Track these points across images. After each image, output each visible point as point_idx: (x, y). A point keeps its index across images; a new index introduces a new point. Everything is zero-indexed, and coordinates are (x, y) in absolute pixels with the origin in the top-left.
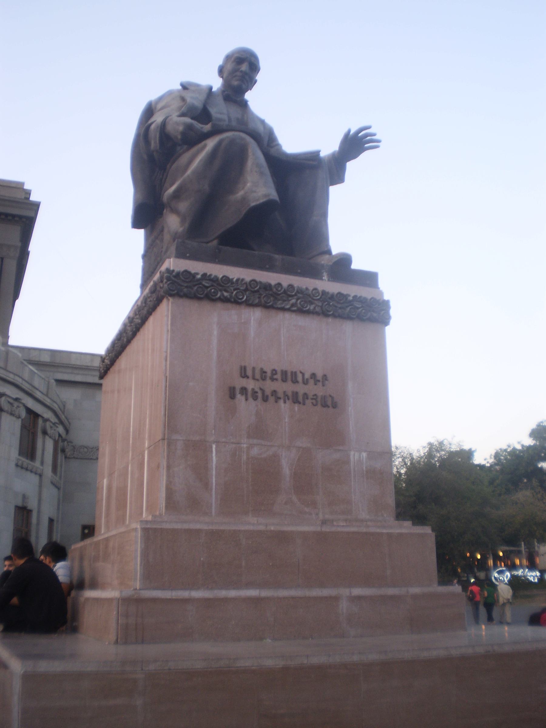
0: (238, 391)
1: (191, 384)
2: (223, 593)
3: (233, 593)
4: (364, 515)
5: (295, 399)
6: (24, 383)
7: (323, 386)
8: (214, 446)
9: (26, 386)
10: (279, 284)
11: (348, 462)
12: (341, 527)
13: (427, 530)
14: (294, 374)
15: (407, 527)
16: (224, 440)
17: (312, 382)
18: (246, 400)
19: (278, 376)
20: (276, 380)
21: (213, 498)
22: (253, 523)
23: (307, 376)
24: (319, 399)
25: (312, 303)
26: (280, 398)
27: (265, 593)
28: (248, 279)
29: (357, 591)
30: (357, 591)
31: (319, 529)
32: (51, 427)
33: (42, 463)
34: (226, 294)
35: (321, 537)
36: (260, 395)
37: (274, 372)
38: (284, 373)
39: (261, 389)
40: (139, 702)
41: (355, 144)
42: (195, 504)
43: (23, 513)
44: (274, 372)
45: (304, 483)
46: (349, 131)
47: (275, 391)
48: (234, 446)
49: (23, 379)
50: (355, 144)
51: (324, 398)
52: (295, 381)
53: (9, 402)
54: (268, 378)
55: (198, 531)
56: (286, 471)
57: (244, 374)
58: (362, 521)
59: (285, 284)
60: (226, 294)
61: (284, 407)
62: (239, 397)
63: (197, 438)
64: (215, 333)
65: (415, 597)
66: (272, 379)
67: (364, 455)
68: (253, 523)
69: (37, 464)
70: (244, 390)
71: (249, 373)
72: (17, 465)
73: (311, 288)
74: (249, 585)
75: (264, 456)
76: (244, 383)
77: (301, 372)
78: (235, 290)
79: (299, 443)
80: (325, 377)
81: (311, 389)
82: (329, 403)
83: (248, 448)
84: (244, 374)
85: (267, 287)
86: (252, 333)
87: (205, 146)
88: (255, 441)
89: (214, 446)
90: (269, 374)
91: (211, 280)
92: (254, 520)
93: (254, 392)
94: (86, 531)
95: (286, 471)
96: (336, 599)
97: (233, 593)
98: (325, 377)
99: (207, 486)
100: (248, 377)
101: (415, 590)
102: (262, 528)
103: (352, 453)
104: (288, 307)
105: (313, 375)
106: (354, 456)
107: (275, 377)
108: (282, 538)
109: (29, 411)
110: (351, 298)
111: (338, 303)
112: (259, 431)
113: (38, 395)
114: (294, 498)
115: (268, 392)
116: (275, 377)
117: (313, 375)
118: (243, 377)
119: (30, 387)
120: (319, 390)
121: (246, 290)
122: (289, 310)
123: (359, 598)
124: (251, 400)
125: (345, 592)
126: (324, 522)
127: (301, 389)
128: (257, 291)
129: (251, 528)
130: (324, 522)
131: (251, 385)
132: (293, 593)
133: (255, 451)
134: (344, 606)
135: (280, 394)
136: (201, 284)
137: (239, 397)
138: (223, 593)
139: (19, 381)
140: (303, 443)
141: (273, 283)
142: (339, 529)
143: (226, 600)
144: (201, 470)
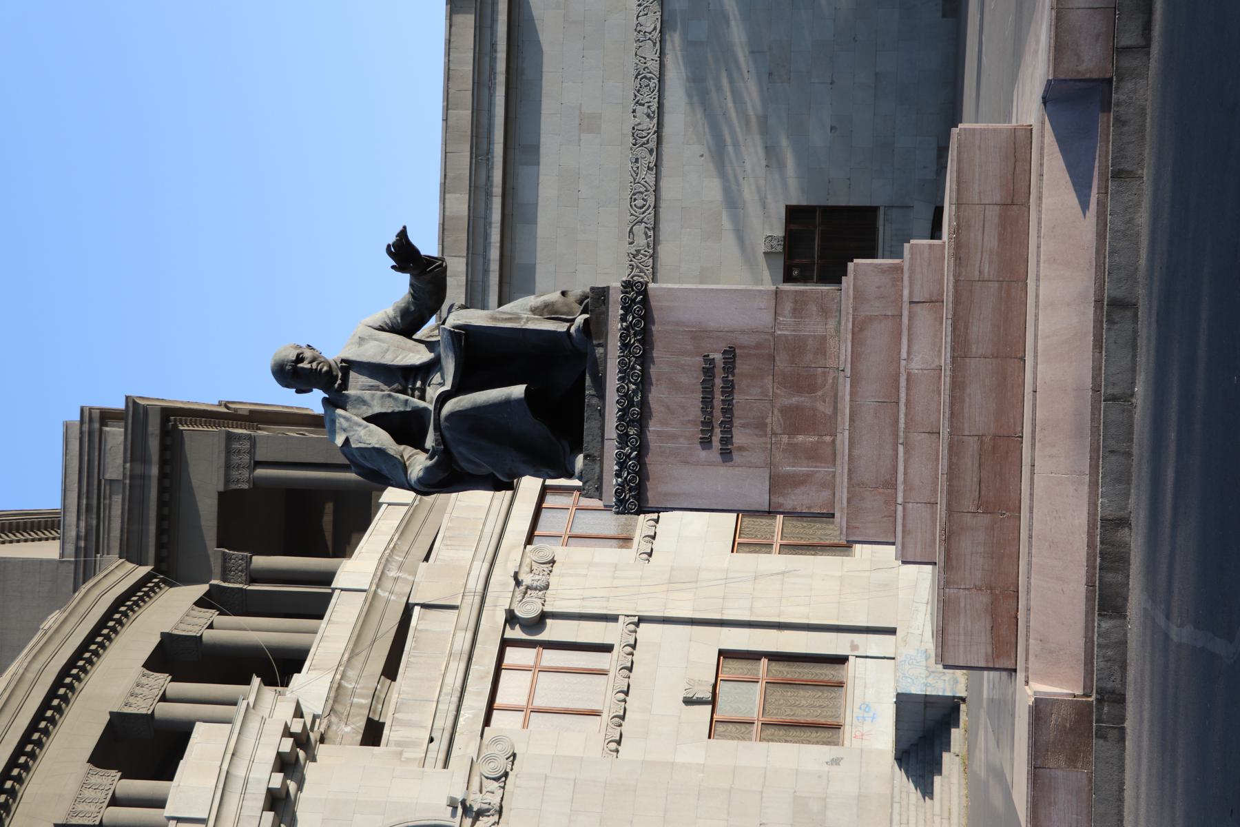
5: (729, 388)
12: (846, 349)
21: (822, 470)
22: (843, 438)
29: (904, 355)
31: (848, 380)
56: (794, 400)
88: (769, 429)
94: (795, 273)
95: (794, 400)
96: (909, 375)
102: (847, 433)
112: (760, 426)
114: (820, 393)
123: (909, 353)
127: (718, 382)
140: (768, 381)
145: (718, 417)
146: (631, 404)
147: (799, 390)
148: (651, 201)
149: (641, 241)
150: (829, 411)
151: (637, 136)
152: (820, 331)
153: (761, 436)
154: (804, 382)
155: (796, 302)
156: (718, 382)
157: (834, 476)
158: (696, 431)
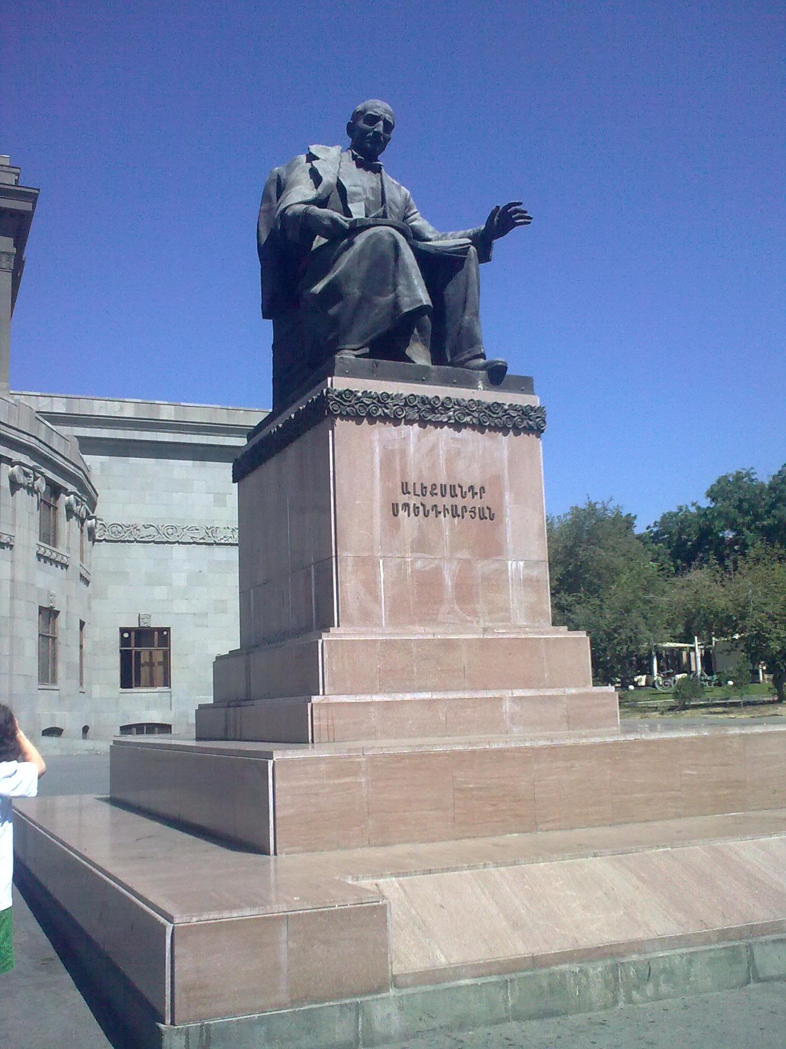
0: (400, 509)
1: (357, 502)
2: (399, 697)
3: (408, 697)
4: (522, 622)
6: (42, 445)
7: (481, 498)
8: (381, 561)
9: (45, 450)
10: (437, 397)
11: (507, 571)
12: (502, 633)
13: (582, 634)
14: (453, 487)
15: (563, 632)
16: (390, 555)
17: (470, 494)
18: (409, 515)
19: (438, 491)
20: (436, 494)
22: (420, 633)
23: (465, 489)
24: (477, 511)
25: (469, 415)
26: (440, 513)
27: (436, 696)
28: (406, 394)
29: (518, 693)
30: (518, 693)
31: (481, 636)
32: (77, 502)
33: (68, 548)
34: (386, 411)
35: (484, 644)
36: (421, 508)
37: (434, 486)
38: (443, 487)
39: (422, 505)
40: (363, 780)
41: (504, 221)
42: (367, 617)
43: (49, 614)
44: (434, 486)
45: (465, 593)
46: (498, 207)
47: (436, 506)
48: (399, 560)
49: (40, 441)
50: (504, 221)
51: (481, 510)
52: (454, 495)
53: (24, 472)
54: (428, 493)
55: (375, 641)
56: (448, 581)
57: (405, 492)
58: (520, 627)
59: (442, 397)
60: (386, 411)
61: (445, 520)
62: (402, 514)
63: (366, 554)
64: (377, 450)
65: (572, 697)
66: (432, 494)
67: (521, 564)
68: (420, 633)
69: (61, 549)
70: (406, 506)
71: (411, 489)
72: (38, 555)
73: (467, 399)
74: (420, 689)
75: (428, 568)
76: (404, 499)
77: (461, 487)
78: (394, 405)
79: (459, 556)
80: (482, 489)
81: (469, 502)
82: (487, 515)
83: (413, 562)
84: (405, 492)
85: (424, 400)
86: (412, 449)
87: (351, 244)
88: (419, 555)
89: (381, 561)
90: (429, 489)
91: (371, 397)
92: (421, 629)
93: (416, 508)
94: (126, 635)
95: (448, 581)
97: (408, 697)
98: (482, 489)
99: (376, 599)
100: (409, 493)
101: (573, 691)
102: (430, 637)
103: (510, 563)
104: (445, 420)
105: (471, 488)
106: (511, 565)
107: (435, 492)
108: (449, 645)
109: (49, 482)
110: (506, 407)
111: (494, 413)
112: (421, 545)
113: (59, 460)
114: (457, 608)
115: (428, 507)
116: (435, 492)
117: (471, 488)
118: (404, 494)
119: (50, 451)
120: (477, 502)
121: (406, 405)
122: (446, 423)
124: (412, 514)
125: (508, 694)
126: (485, 630)
127: (459, 502)
128: (416, 406)
129: (421, 637)
130: (485, 630)
131: (413, 501)
132: (460, 695)
133: (419, 564)
134: (507, 706)
135: (440, 509)
136: (362, 402)
137: (402, 514)
138: (399, 697)
139: (33, 442)
140: (464, 554)
141: (430, 396)
142: (501, 636)
143: (403, 702)
144: (370, 585)
145: (429, 501)
146: (433, 410)
147: (458, 586)
148: (171, 539)
149: (144, 533)
150: (440, 618)
151: (214, 530)
152: (514, 605)
153: (412, 548)
154: (465, 593)
155: (538, 581)
156: (459, 502)
157: (376, 625)
158: (412, 478)
